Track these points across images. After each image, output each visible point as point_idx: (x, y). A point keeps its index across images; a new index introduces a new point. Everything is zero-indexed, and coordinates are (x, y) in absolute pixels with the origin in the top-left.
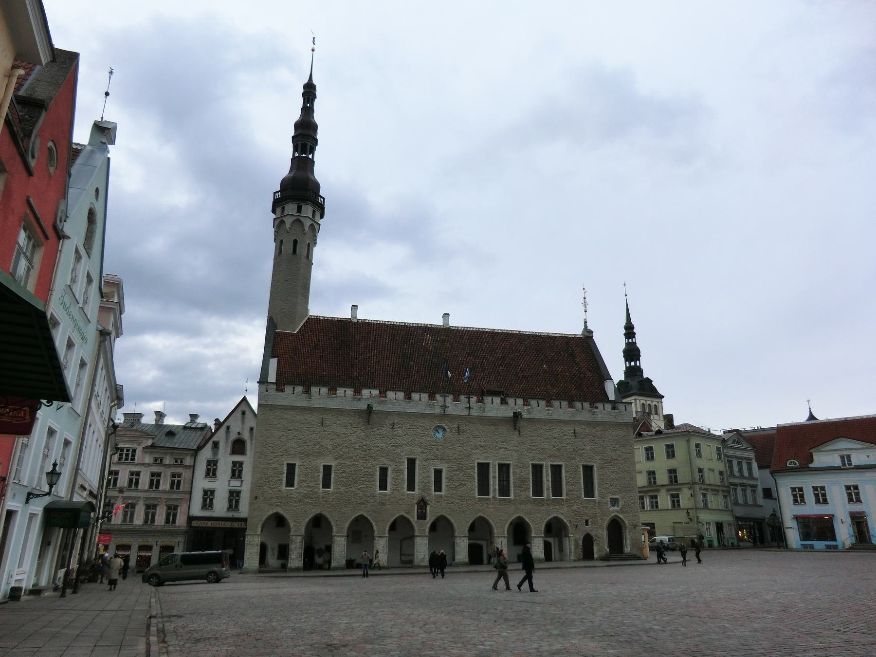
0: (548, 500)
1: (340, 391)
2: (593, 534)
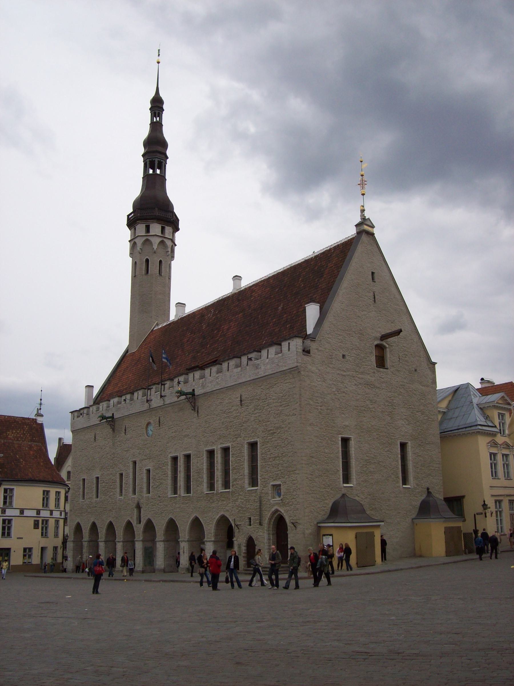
0: (217, 494)
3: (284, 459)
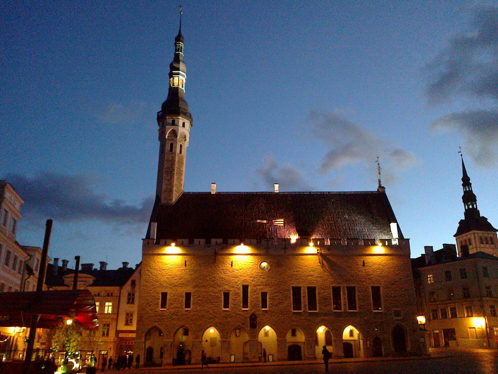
0: (345, 312)
1: (196, 241)
2: (380, 337)
3: (403, 298)
